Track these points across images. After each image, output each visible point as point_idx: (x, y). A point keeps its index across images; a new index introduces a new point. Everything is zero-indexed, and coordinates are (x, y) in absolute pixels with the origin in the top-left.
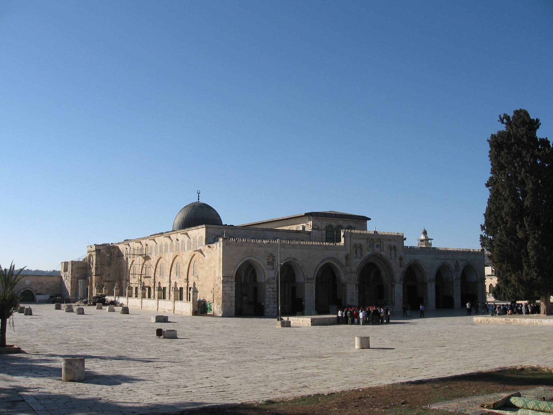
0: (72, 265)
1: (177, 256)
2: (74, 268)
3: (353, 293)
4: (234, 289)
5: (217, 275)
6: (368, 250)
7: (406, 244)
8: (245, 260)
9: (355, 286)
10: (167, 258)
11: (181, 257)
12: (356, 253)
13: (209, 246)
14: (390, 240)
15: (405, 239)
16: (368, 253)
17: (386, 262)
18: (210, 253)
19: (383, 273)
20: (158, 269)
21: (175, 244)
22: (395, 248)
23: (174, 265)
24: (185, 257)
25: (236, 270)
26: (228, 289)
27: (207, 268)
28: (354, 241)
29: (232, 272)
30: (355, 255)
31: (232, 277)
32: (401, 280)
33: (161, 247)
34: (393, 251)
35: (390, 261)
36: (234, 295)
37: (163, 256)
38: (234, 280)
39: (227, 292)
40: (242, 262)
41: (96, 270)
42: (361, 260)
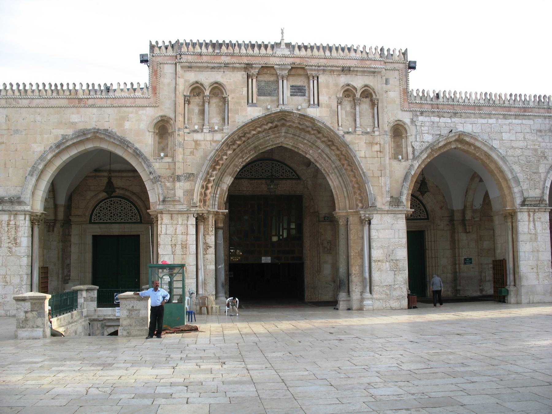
3: (184, 246)
6: (250, 103)
7: (418, 82)
9: (193, 221)
12: (202, 112)
14: (346, 70)
15: (412, 66)
16: (254, 113)
17: (332, 141)
19: (334, 182)
22: (367, 93)
28: (192, 77)
30: (196, 118)
32: (396, 201)
34: (365, 106)
35: (348, 138)
42: (218, 137)
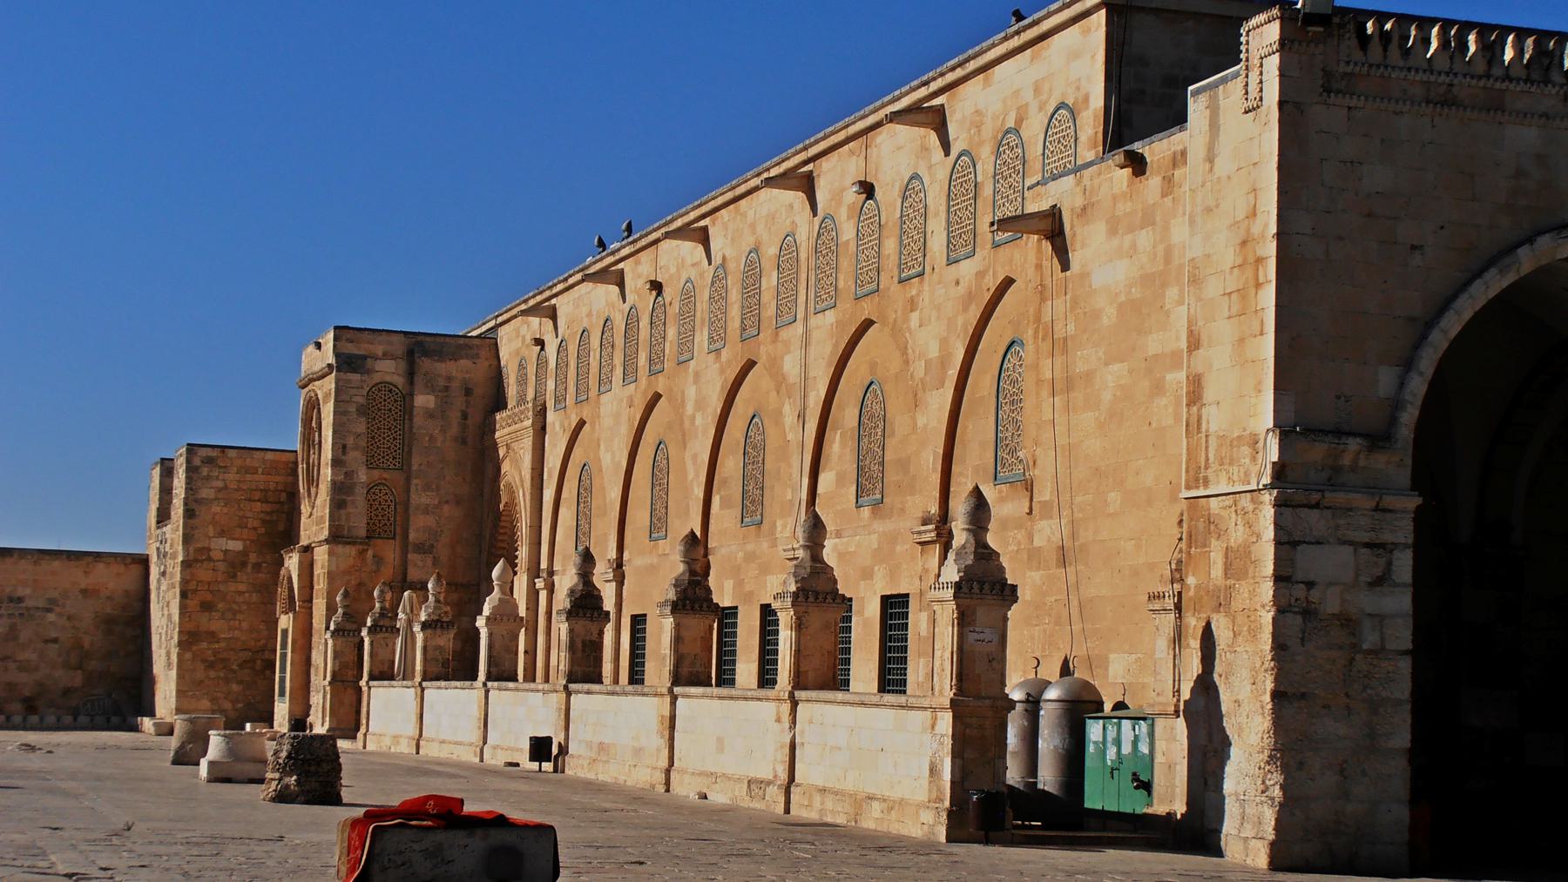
0: (191, 469)
1: (867, 324)
4: (1404, 565)
5: (1215, 419)
8: (1527, 261)
10: (791, 366)
11: (898, 334)
13: (1137, 164)
18: (1148, 220)
20: (730, 465)
21: (848, 232)
23: (846, 414)
24: (932, 327)
25: (1427, 362)
26: (1331, 564)
27: (1113, 376)
29: (1386, 379)
31: (1379, 439)
33: (753, 273)
36: (1402, 636)
37: (763, 353)
38: (1404, 477)
39: (1332, 606)
40: (1494, 284)
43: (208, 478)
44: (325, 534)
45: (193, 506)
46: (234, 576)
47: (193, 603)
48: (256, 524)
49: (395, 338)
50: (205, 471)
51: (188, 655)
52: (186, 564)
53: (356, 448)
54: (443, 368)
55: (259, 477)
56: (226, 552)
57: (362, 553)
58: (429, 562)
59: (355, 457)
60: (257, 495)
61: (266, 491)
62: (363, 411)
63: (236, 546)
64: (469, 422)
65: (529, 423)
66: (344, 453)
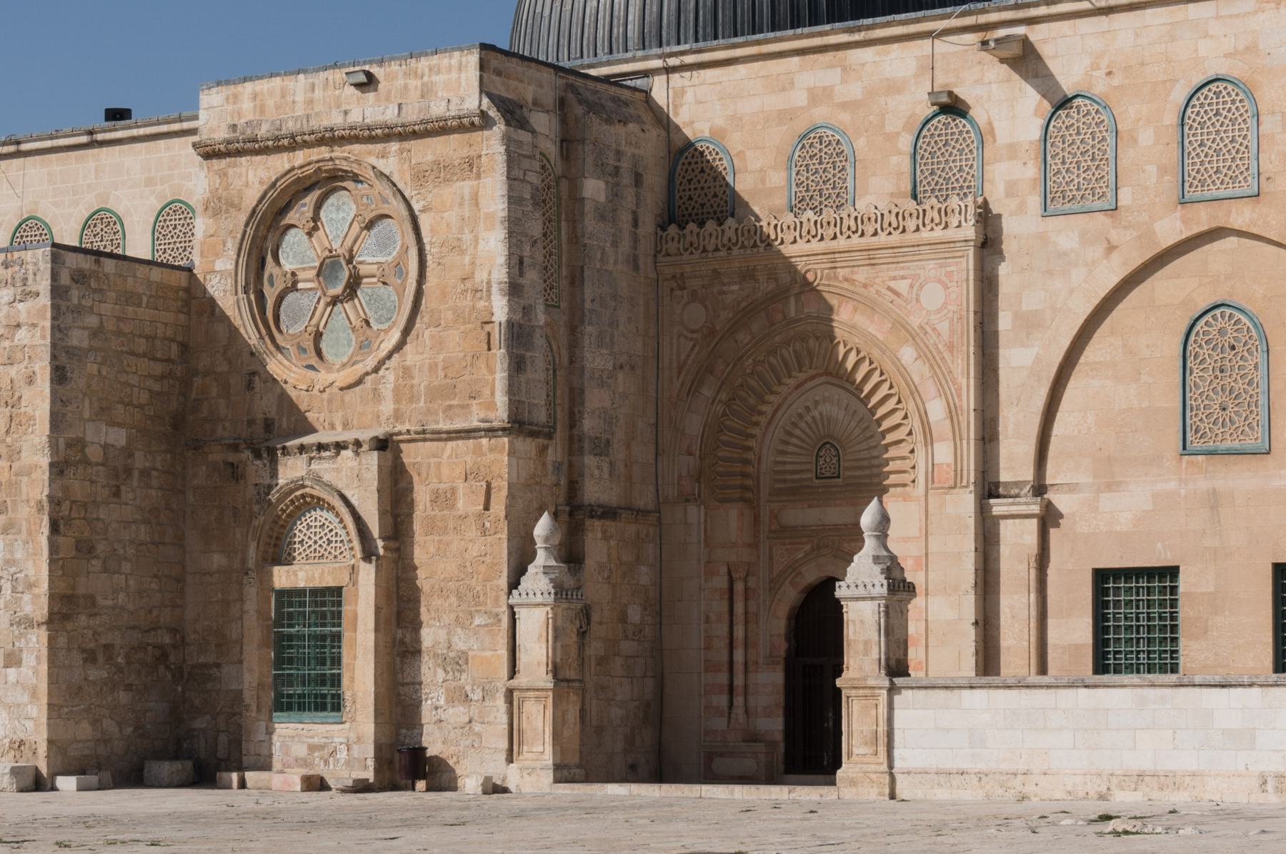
2: (78, 338)
41: (517, 365)
43: (78, 310)
44: (500, 414)
45: (63, 359)
46: (117, 494)
47: (66, 542)
48: (144, 397)
49: (547, 75)
50: (75, 295)
51: (62, 641)
52: (58, 469)
53: (533, 266)
54: (615, 134)
55: (145, 313)
56: (106, 447)
57: (545, 448)
58: (606, 467)
59: (532, 276)
60: (141, 345)
61: (151, 338)
62: (539, 202)
63: (118, 437)
64: (641, 231)
65: (969, 231)
66: (521, 274)
